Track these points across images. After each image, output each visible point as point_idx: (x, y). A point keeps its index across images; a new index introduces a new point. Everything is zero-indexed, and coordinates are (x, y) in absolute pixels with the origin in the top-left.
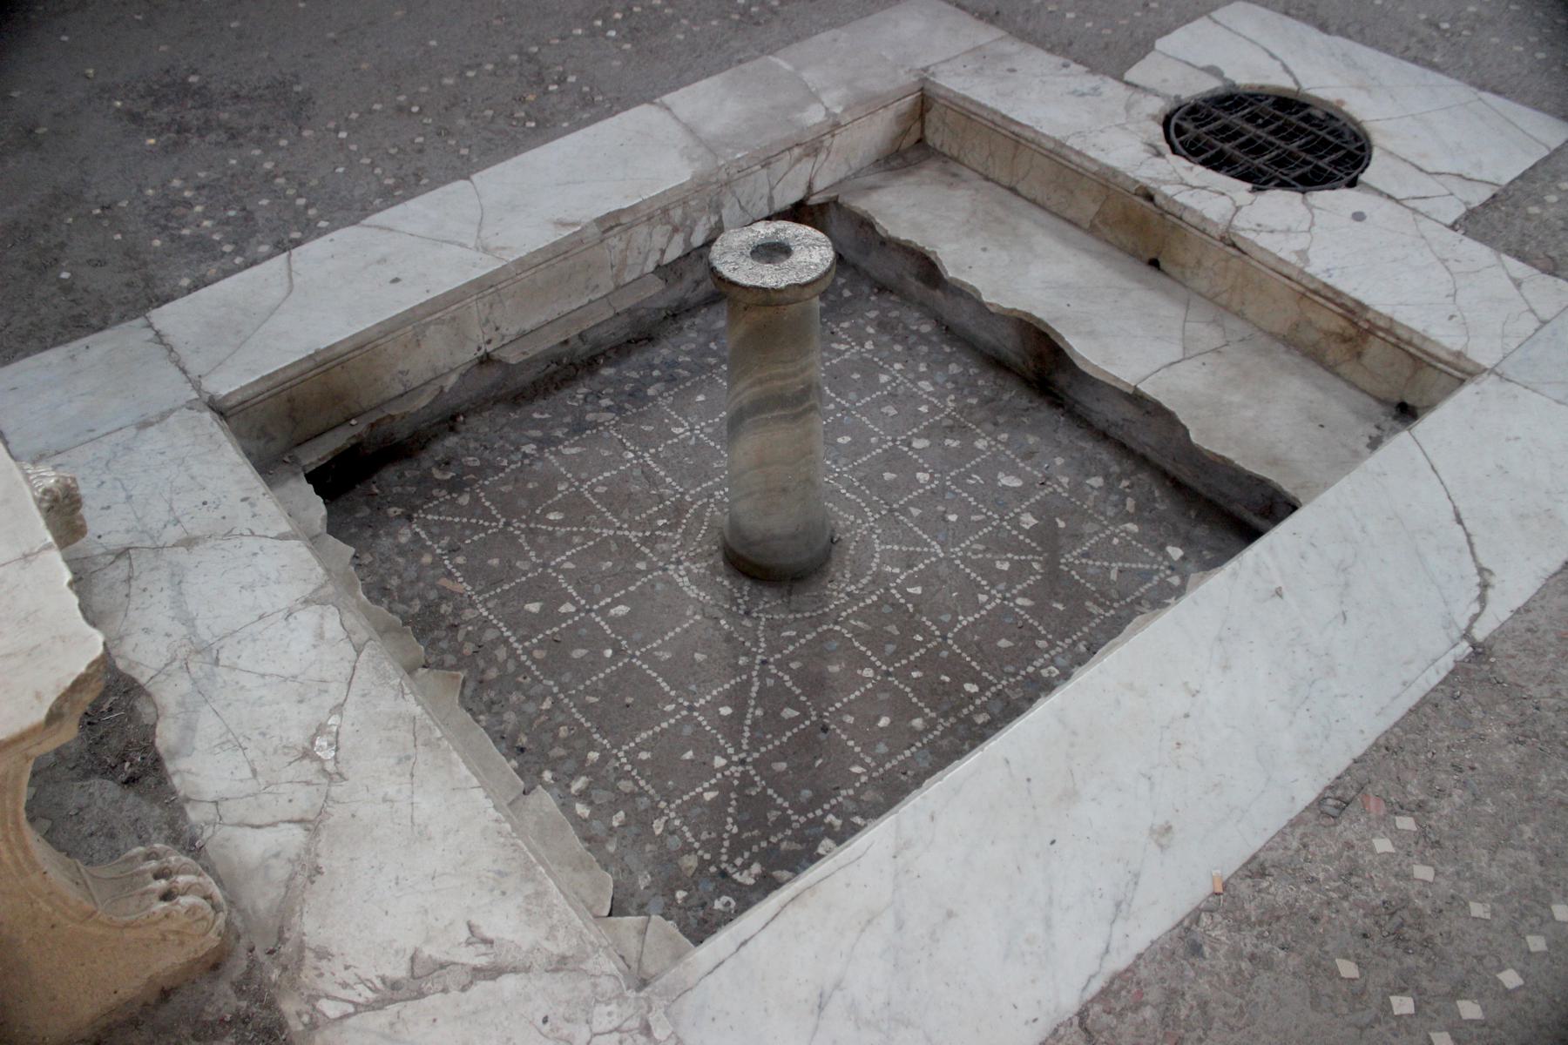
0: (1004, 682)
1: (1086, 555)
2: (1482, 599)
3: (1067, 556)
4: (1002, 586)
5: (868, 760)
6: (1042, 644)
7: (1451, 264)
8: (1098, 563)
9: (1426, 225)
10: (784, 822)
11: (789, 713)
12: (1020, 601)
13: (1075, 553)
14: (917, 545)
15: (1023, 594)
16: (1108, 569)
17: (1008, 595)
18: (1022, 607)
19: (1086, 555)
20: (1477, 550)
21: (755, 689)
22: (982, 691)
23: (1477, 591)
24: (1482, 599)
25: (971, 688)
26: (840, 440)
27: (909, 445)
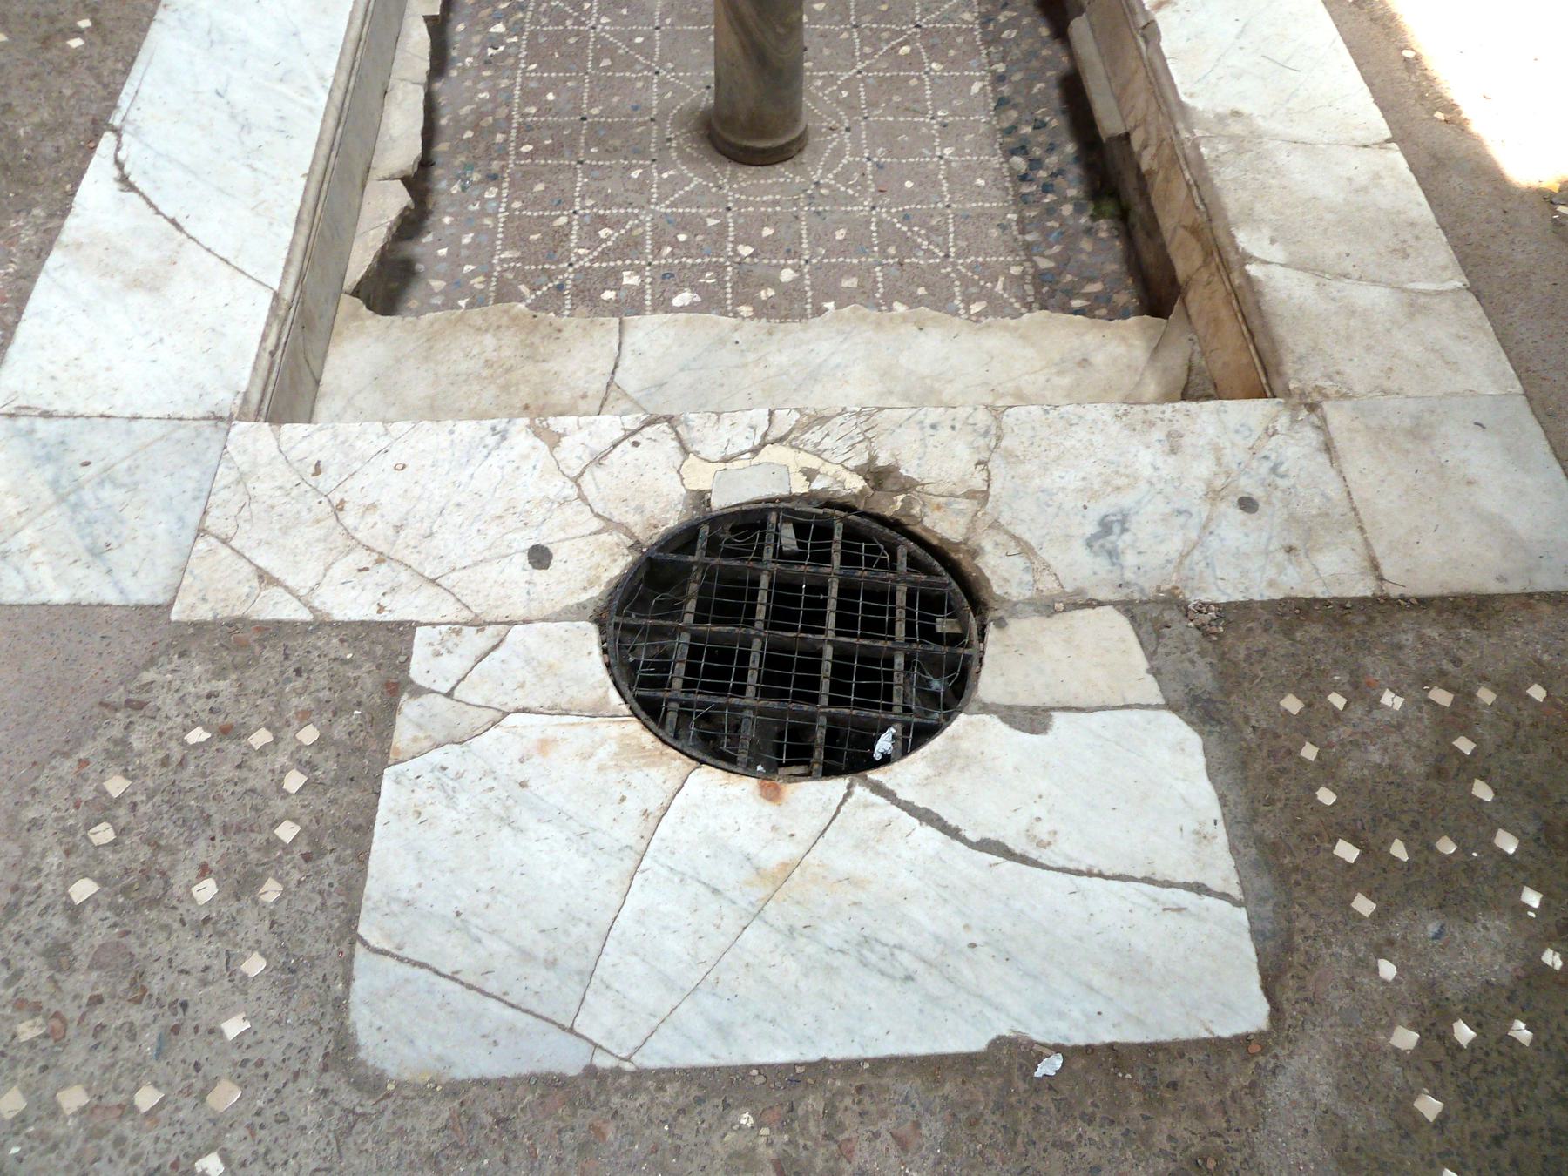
0: (511, 166)
1: (561, 287)
2: (119, 164)
3: (572, 276)
4: (587, 220)
5: (533, 75)
6: (517, 205)
7: (366, 559)
8: (545, 289)
9: (450, 611)
10: (533, 22)
11: (606, 62)
12: (563, 220)
13: (569, 282)
14: (672, 202)
15: (569, 223)
16: (533, 290)
17: (576, 217)
18: (558, 216)
19: (561, 287)
20: (142, 203)
21: (641, 59)
22: (519, 155)
23: (127, 169)
24: (119, 164)
25: (527, 148)
26: (843, 231)
27: (792, 267)
